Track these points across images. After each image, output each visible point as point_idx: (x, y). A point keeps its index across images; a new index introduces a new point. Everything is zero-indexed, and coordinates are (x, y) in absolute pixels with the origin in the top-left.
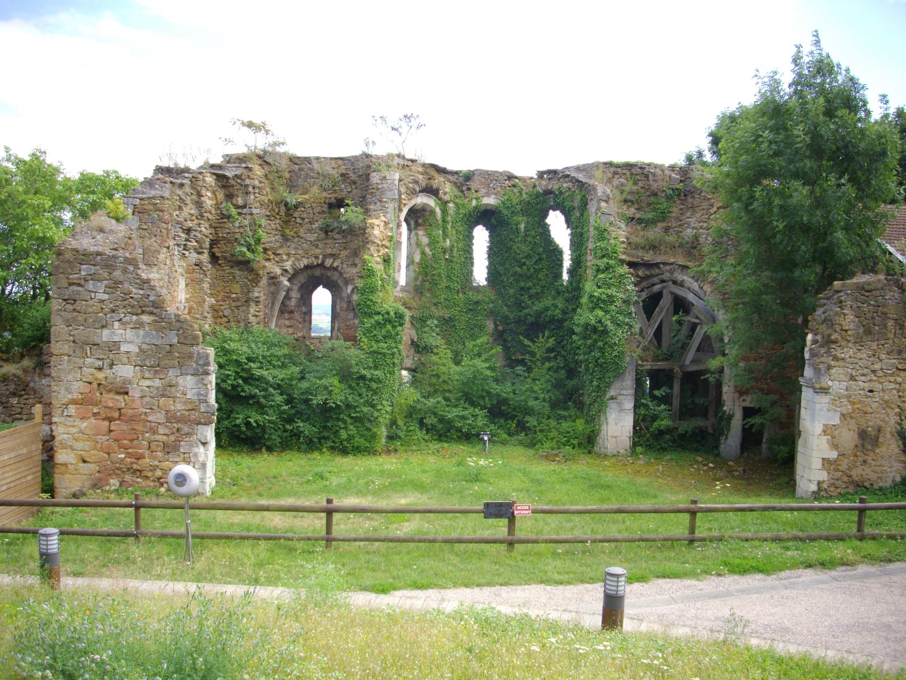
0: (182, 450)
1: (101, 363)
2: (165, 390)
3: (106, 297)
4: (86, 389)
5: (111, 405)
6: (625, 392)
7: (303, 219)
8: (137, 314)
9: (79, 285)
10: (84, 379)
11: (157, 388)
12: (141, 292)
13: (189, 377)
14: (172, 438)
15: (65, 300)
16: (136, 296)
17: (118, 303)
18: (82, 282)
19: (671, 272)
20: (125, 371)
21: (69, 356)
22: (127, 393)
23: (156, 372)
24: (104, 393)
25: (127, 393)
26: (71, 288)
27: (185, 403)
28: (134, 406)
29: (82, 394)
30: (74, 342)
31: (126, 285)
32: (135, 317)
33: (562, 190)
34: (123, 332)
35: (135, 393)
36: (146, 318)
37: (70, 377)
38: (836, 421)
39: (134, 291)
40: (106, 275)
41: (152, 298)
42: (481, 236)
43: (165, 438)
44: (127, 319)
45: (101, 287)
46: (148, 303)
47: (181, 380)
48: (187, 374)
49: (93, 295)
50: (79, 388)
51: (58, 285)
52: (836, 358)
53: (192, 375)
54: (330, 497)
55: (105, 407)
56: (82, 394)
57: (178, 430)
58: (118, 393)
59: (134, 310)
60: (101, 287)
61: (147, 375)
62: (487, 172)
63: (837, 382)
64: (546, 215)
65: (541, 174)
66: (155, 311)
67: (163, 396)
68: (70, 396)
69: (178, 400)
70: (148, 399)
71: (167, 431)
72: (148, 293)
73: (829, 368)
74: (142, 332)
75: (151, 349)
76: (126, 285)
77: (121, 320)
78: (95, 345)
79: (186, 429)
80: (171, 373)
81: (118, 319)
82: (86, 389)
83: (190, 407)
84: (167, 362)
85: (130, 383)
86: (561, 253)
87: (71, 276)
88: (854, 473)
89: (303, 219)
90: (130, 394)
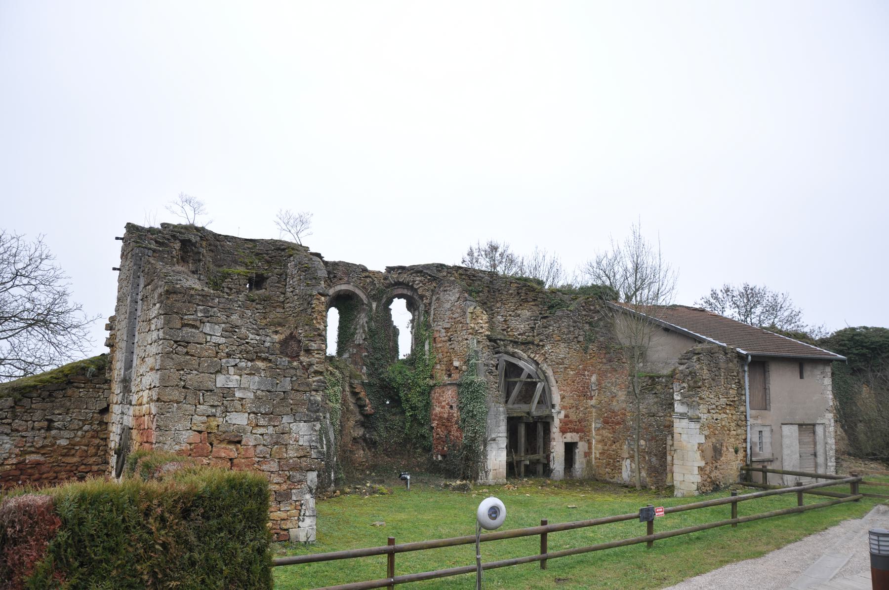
0: (294, 498)
1: (214, 410)
2: (279, 437)
3: (223, 340)
4: (197, 438)
5: (223, 455)
6: (500, 435)
7: (231, 289)
8: (252, 360)
9: (193, 326)
10: (195, 428)
11: (271, 435)
12: (258, 338)
13: (302, 424)
14: (285, 487)
15: (176, 342)
16: (252, 342)
17: (234, 348)
18: (198, 324)
19: (505, 346)
20: (240, 419)
21: (178, 403)
22: (239, 442)
23: (270, 420)
24: (215, 443)
25: (239, 442)
26: (185, 329)
27: (297, 450)
28: (248, 455)
29: (190, 444)
30: (184, 387)
31: (243, 330)
32: (250, 364)
33: (418, 283)
34: (238, 377)
35: (249, 440)
36: (260, 364)
37: (179, 426)
38: (703, 441)
39: (251, 336)
40: (224, 318)
41: (267, 344)
42: (333, 315)
43: (277, 486)
44: (243, 364)
45: (218, 330)
46: (264, 349)
47: (294, 426)
48: (300, 421)
49: (209, 337)
50: (188, 437)
51: (171, 326)
52: (701, 398)
53: (305, 422)
54: (544, 519)
55: (217, 458)
56: (190, 444)
57: (289, 478)
58: (230, 442)
59: (249, 356)
60: (218, 330)
61: (262, 422)
62: (348, 264)
63: (831, 404)
64: (390, 301)
65: (390, 269)
66: (270, 357)
67: (276, 443)
68: (177, 447)
69: (290, 447)
70: (261, 448)
71: (280, 480)
72: (263, 339)
73: (699, 404)
74: (257, 378)
75: (266, 396)
76: (243, 330)
77: (236, 365)
78: (207, 391)
79: (298, 476)
80: (286, 419)
81: (233, 364)
82: (197, 438)
83: (302, 454)
84: (282, 409)
85: (244, 431)
86: (396, 332)
87: (186, 317)
88: (712, 475)
89: (231, 289)
90: (243, 443)
